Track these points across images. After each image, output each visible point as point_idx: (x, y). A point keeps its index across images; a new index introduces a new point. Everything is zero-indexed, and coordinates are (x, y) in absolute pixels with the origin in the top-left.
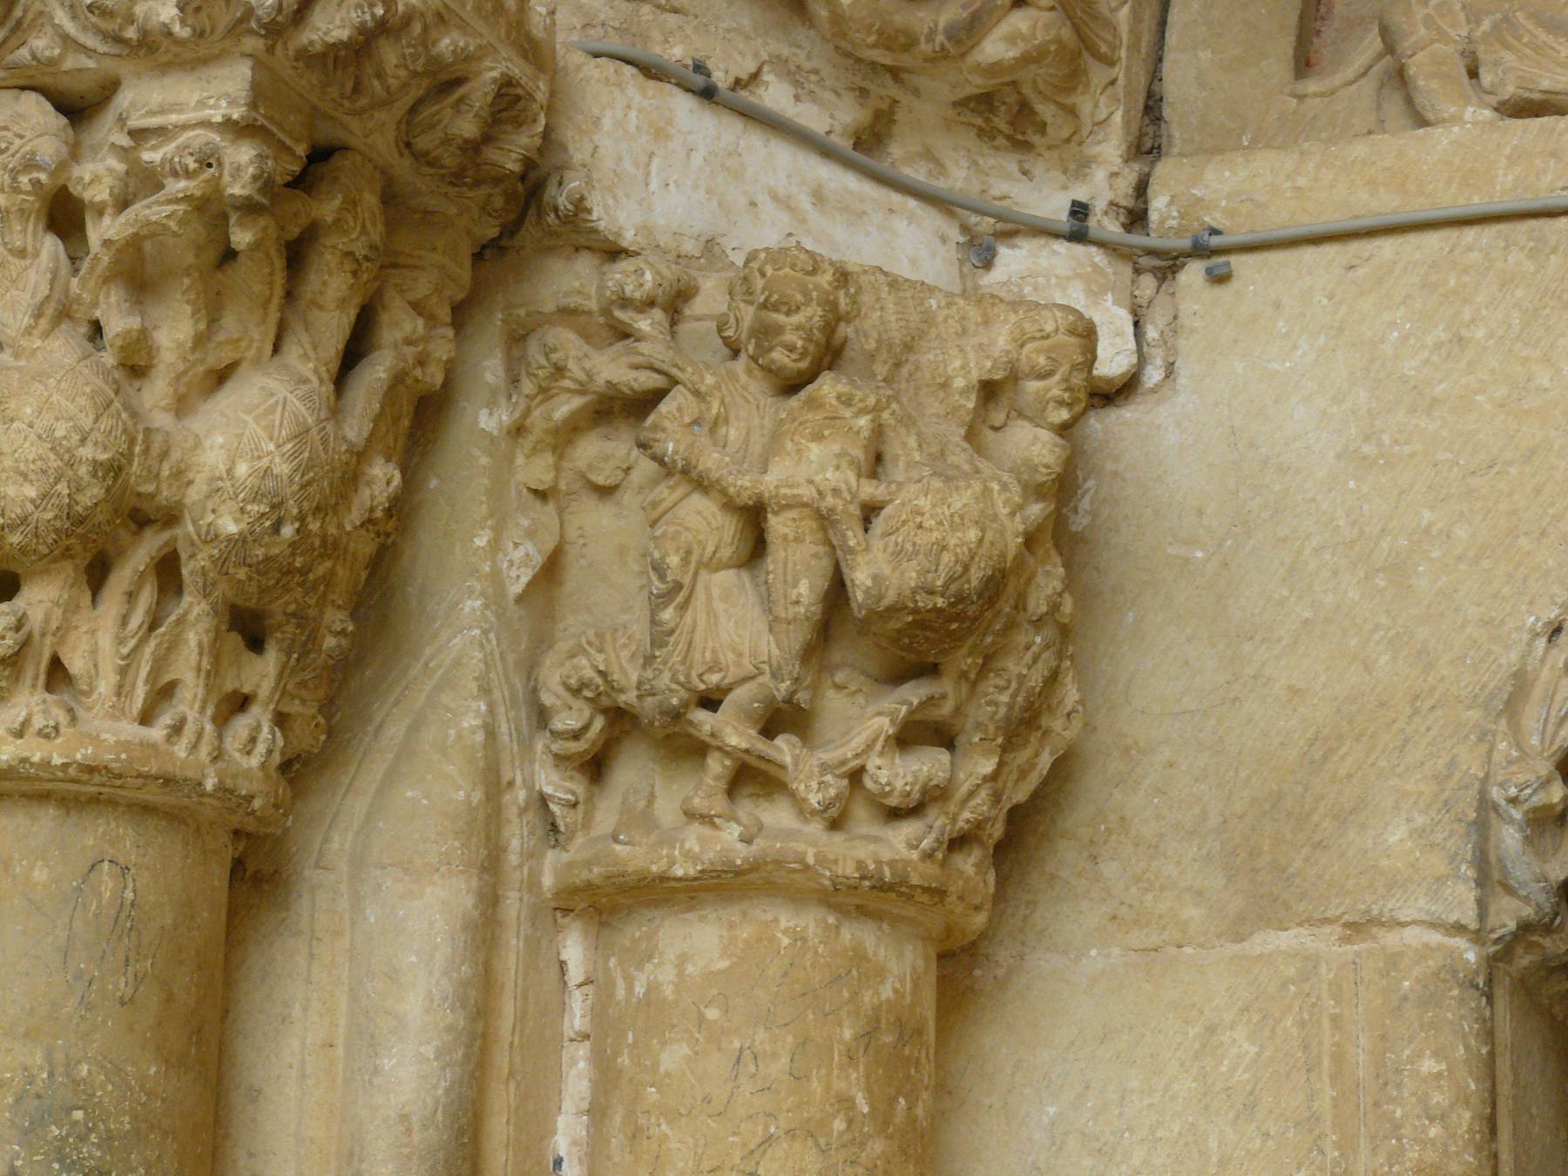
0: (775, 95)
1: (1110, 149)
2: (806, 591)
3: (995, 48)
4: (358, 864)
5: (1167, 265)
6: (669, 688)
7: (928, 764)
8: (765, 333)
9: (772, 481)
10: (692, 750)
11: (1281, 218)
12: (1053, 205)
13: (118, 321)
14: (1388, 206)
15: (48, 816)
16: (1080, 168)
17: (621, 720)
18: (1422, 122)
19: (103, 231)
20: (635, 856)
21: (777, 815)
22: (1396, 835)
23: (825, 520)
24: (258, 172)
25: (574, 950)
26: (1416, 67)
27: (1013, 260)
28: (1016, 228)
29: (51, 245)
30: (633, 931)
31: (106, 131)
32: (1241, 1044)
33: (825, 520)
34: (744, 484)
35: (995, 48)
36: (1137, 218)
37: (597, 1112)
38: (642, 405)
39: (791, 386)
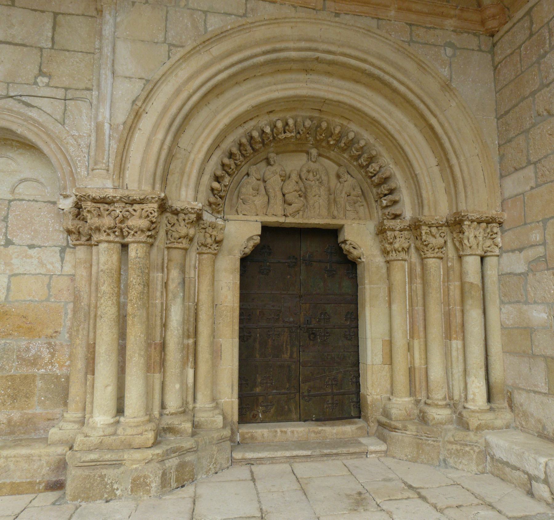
0: (209, 211)
1: (222, 214)
2: (213, 239)
3: (220, 209)
4: (190, 251)
5: (225, 220)
6: (206, 243)
7: (217, 248)
8: (212, 226)
9: (213, 233)
10: (207, 246)
11: (231, 219)
12: (219, 217)
13: (187, 226)
14: (236, 219)
15: (181, 250)
16: (221, 215)
17: (202, 244)
18: (238, 214)
19: (186, 221)
20: (203, 251)
21: (210, 250)
22: (236, 251)
23: (215, 236)
24: (167, 206)
25: (197, 256)
26: (239, 212)
27: (218, 219)
28: (218, 218)
29: (183, 221)
30: (201, 255)
31: (187, 216)
32: (228, 261)
33: (215, 236)
34: (211, 234)
35: (220, 209)
36: (223, 217)
37: (199, 264)
38: (205, 229)
39: (213, 229)
